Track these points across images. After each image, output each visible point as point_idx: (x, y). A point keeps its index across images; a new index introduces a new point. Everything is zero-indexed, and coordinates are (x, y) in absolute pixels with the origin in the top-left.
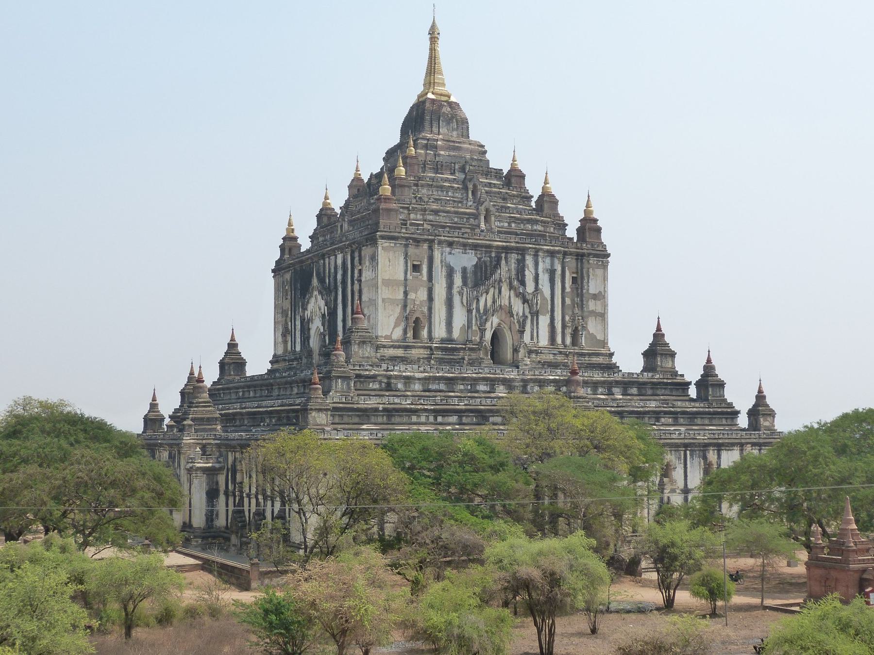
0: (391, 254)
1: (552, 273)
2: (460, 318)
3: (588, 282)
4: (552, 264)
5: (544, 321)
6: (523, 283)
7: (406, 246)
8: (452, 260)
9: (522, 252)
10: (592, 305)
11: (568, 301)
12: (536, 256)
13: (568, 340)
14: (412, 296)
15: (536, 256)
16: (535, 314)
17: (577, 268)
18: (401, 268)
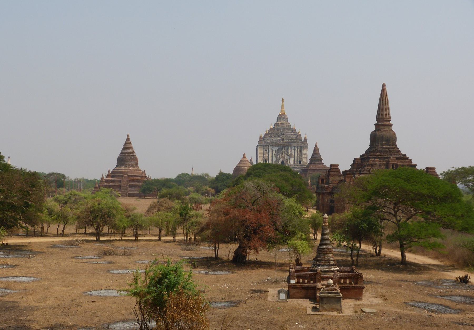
1: (295, 150)
2: (274, 159)
5: (293, 159)
6: (288, 152)
9: (288, 146)
10: (304, 156)
12: (291, 147)
15: (291, 147)
16: (290, 158)
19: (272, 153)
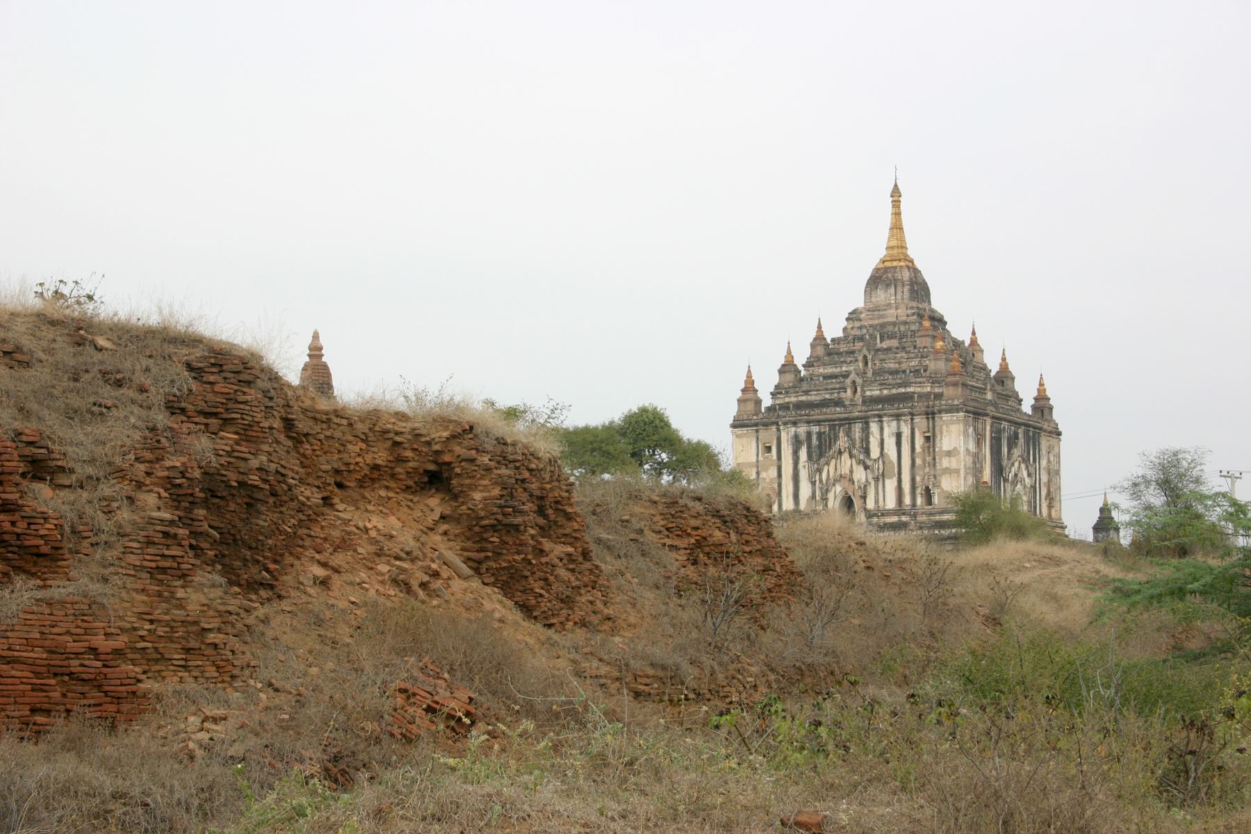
0: (744, 440)
1: (899, 436)
2: (805, 490)
4: (899, 427)
6: (867, 451)
7: (757, 431)
10: (945, 463)
11: (918, 461)
14: (763, 475)
16: (880, 478)
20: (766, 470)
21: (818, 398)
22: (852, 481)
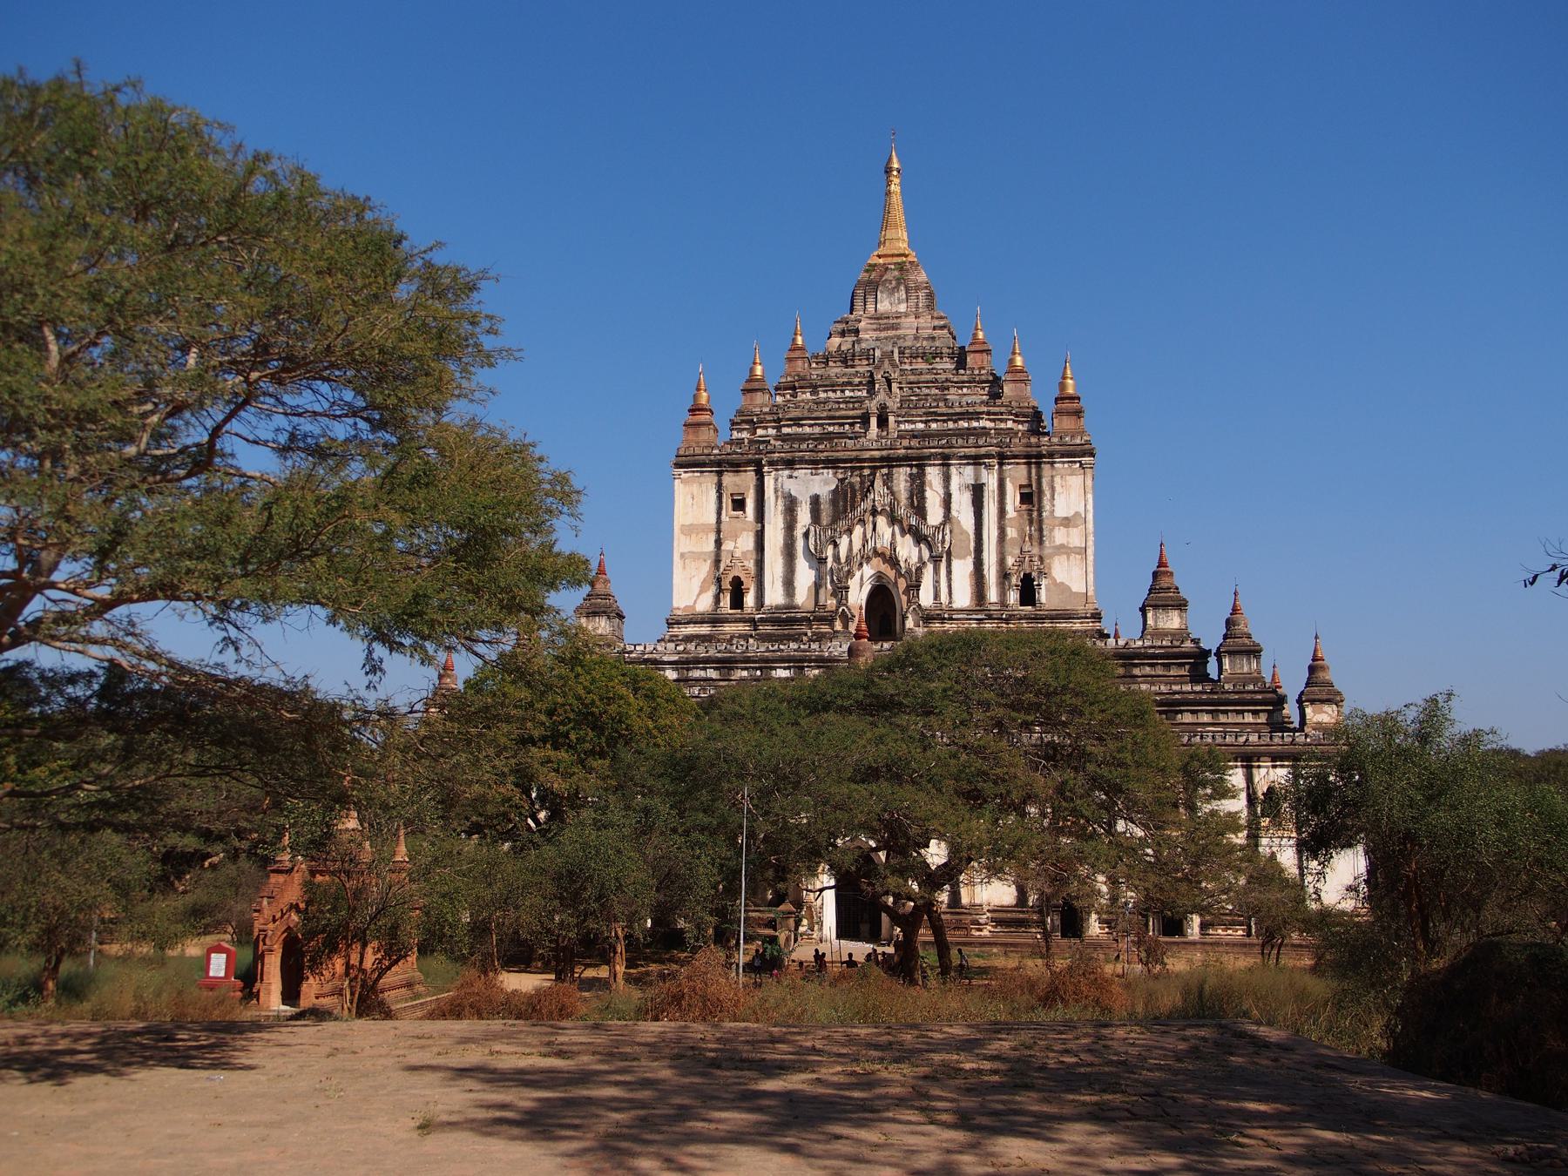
0: (695, 488)
1: (977, 491)
2: (805, 576)
3: (1053, 498)
6: (920, 511)
7: (720, 474)
8: (792, 487)
10: (1059, 536)
11: (1011, 533)
13: (1013, 597)
14: (727, 546)
16: (941, 558)
17: (1030, 477)
18: (713, 506)
19: (790, 527)
20: (735, 538)
21: (817, 430)
22: (893, 561)
